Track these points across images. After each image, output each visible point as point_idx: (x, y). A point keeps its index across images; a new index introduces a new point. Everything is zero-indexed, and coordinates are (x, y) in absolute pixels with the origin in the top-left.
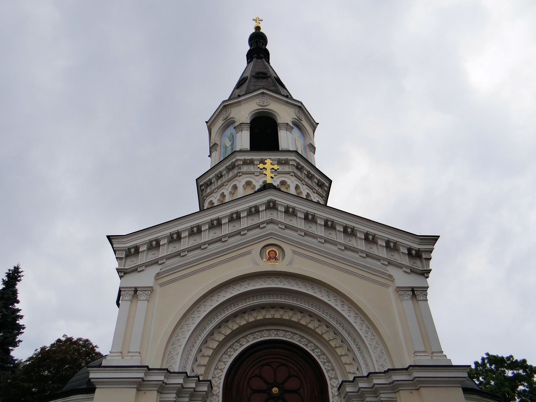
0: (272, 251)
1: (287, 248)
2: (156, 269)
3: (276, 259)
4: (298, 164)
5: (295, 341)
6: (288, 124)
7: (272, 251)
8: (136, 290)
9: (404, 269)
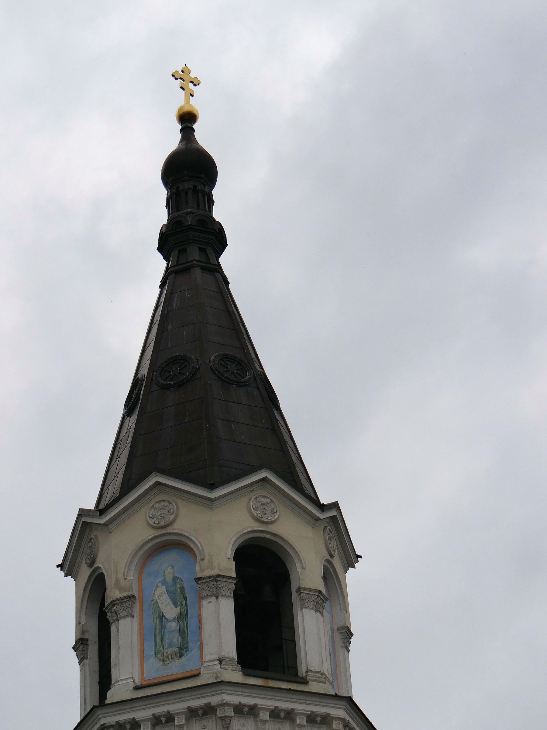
6: (320, 592)
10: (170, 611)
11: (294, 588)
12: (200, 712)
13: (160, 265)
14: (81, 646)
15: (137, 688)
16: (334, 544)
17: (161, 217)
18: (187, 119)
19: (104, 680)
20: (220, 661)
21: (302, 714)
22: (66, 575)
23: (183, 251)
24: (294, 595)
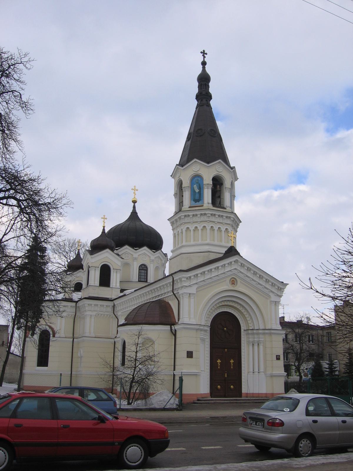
0: (233, 282)
1: (239, 280)
2: (196, 286)
3: (234, 284)
4: (234, 219)
5: (232, 312)
7: (233, 282)
8: (190, 294)
9: (275, 294)
10: (197, 191)
11: (224, 187)
12: (203, 214)
13: (195, 103)
14: (175, 195)
15: (189, 207)
16: (233, 176)
17: (196, 91)
18: (204, 64)
19: (180, 204)
20: (208, 203)
21: (225, 216)
22: (172, 178)
23: (202, 100)
24: (224, 189)
